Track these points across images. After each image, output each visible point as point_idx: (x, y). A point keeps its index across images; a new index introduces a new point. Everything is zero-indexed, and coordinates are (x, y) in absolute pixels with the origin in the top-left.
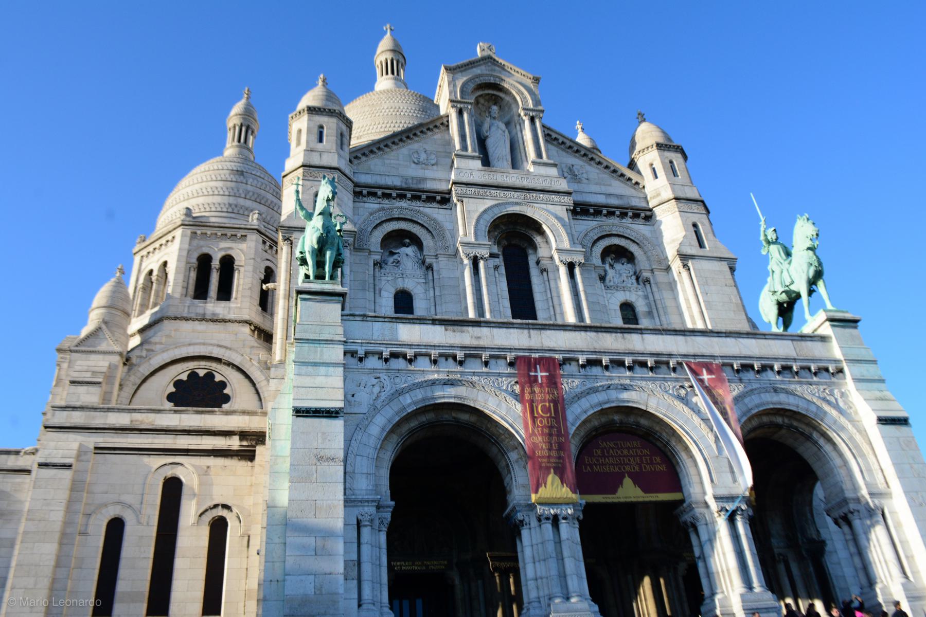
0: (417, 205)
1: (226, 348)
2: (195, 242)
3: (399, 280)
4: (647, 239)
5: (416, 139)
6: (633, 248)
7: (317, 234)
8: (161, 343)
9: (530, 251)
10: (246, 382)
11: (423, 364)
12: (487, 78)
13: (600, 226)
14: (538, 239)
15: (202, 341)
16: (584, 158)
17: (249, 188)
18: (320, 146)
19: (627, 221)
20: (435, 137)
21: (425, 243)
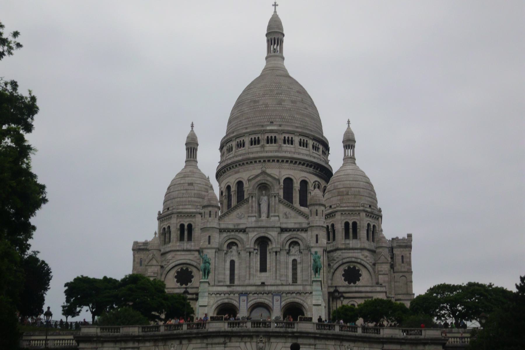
0: (237, 233)
1: (191, 260)
2: (178, 220)
3: (232, 257)
4: (304, 238)
5: (238, 208)
6: (300, 242)
7: (203, 268)
8: (171, 260)
9: (268, 246)
10: (198, 271)
11: (222, 295)
12: (262, 181)
13: (290, 235)
14: (269, 243)
15: (183, 258)
16: (291, 208)
17: (196, 192)
18: (210, 219)
19: (299, 233)
20: (245, 206)
21: (239, 246)
